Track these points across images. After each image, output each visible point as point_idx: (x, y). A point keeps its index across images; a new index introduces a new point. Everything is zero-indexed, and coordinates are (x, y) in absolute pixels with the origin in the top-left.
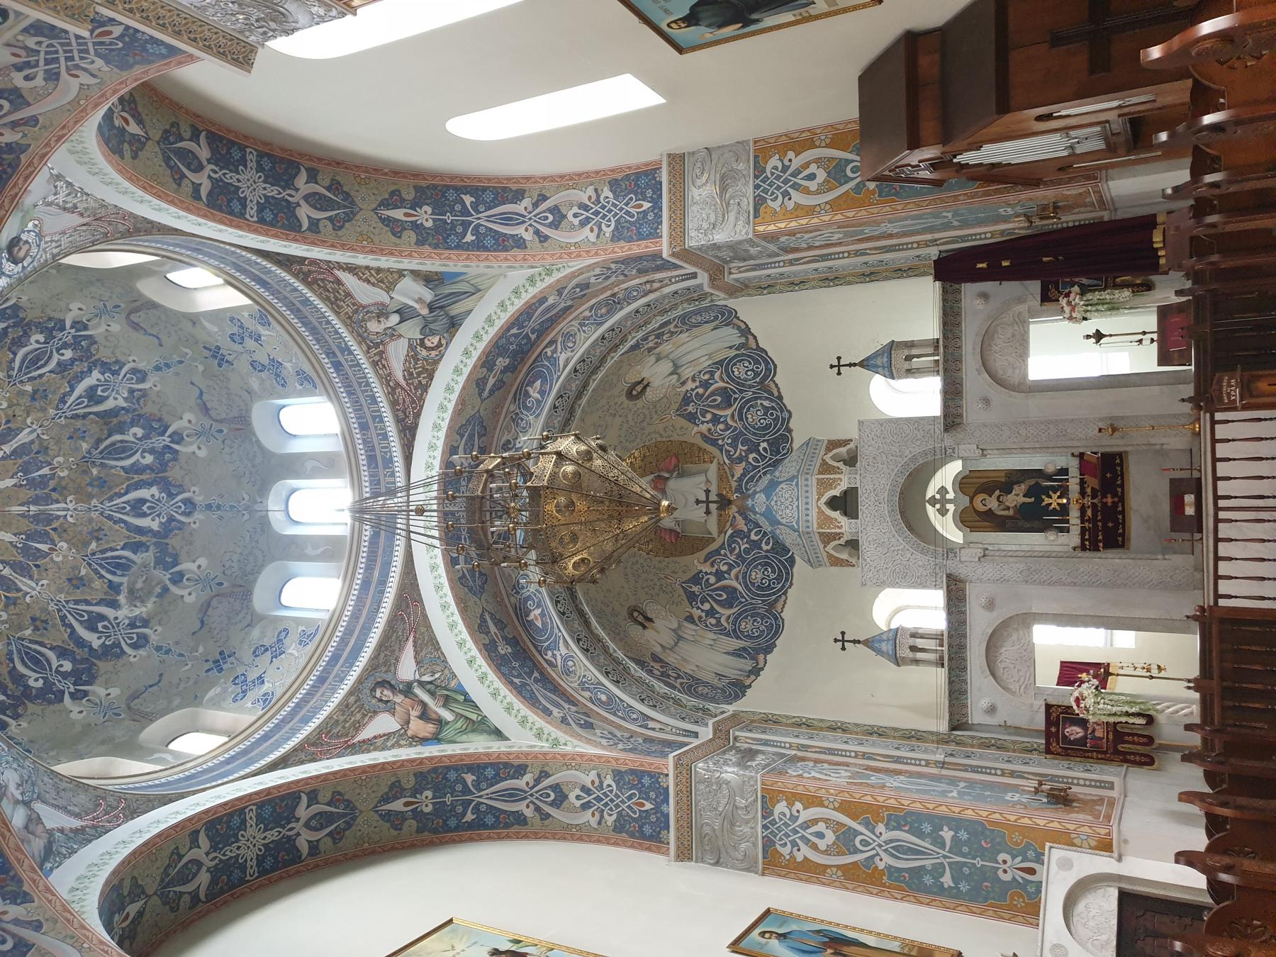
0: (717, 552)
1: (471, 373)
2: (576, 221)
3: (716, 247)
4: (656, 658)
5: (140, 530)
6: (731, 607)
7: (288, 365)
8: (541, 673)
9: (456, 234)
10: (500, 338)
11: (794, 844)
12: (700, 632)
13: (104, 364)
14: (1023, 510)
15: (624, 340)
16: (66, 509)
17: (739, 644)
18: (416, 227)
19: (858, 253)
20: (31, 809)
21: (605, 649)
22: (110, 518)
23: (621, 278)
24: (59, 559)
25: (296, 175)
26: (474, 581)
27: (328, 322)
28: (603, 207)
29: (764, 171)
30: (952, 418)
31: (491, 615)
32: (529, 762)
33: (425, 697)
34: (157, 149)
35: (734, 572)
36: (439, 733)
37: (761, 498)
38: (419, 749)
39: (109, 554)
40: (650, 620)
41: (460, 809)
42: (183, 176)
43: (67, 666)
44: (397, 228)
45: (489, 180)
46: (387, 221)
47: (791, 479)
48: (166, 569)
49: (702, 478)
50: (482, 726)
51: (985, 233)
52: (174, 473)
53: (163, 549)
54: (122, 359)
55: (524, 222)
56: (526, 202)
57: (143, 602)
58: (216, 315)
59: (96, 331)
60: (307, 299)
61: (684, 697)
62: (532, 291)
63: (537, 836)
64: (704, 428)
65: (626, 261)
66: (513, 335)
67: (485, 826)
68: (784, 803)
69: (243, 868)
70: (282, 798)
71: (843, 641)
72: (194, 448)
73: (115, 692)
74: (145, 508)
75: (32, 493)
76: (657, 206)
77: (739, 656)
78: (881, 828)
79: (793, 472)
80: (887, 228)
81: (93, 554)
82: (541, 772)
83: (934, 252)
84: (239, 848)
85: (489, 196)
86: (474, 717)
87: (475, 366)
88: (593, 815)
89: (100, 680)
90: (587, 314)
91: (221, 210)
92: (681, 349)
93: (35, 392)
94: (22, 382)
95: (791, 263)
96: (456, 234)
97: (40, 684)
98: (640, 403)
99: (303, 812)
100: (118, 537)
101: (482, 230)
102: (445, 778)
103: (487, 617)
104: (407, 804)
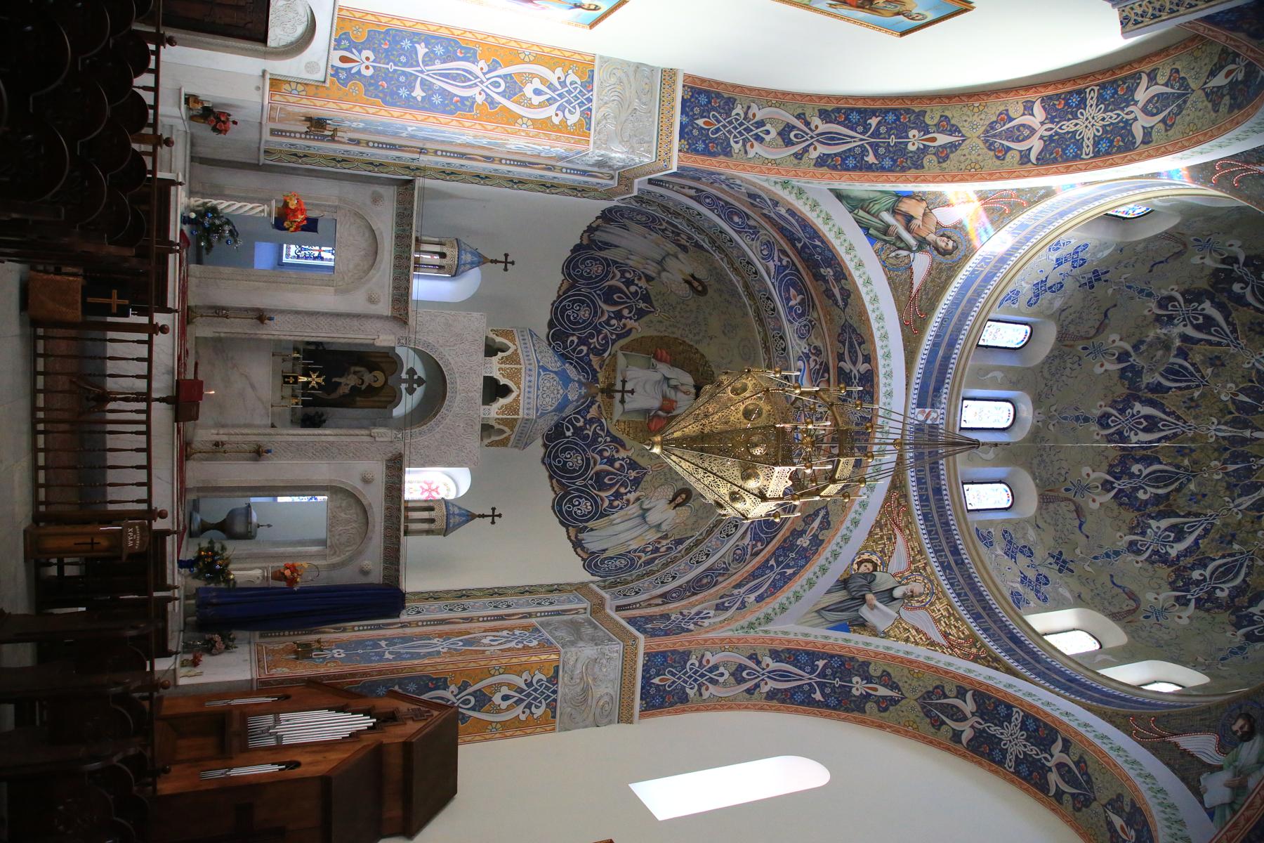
0: (620, 337)
2: (722, 670)
3: (595, 641)
4: (684, 249)
5: (1152, 403)
7: (999, 552)
8: (794, 246)
10: (803, 567)
11: (563, 84)
12: (640, 266)
16: (1215, 430)
17: (603, 254)
18: (868, 679)
19: (469, 620)
21: (731, 263)
22: (1178, 418)
23: (685, 612)
24: (1230, 385)
25: (971, 740)
27: (959, 595)
28: (696, 680)
29: (548, 705)
30: (396, 468)
31: (836, 303)
34: (1097, 795)
35: (604, 318)
37: (572, 396)
40: (687, 282)
41: (883, 130)
42: (1077, 764)
43: (1237, 287)
46: (894, 686)
47: (542, 415)
48: (1132, 366)
49: (628, 406)
53: (1133, 386)
54: (1147, 565)
57: (1158, 338)
58: (1060, 605)
59: (1167, 595)
61: (660, 214)
64: (623, 454)
67: (859, 111)
68: (569, 123)
69: (1101, 99)
70: (1055, 161)
71: (506, 262)
72: (1093, 476)
73: (1196, 260)
74: (1145, 424)
75: (1246, 449)
76: (646, 680)
77: (606, 243)
78: (480, 99)
79: (541, 421)
81: (1198, 386)
83: (404, 617)
84: (1103, 119)
86: (861, 213)
87: (829, 542)
88: (754, 115)
89: (1207, 272)
90: (720, 579)
91: (1045, 724)
92: (639, 532)
93: (1230, 543)
94: (1242, 553)
95: (530, 615)
99: (1036, 145)
100: (1172, 400)
104: (934, 140)
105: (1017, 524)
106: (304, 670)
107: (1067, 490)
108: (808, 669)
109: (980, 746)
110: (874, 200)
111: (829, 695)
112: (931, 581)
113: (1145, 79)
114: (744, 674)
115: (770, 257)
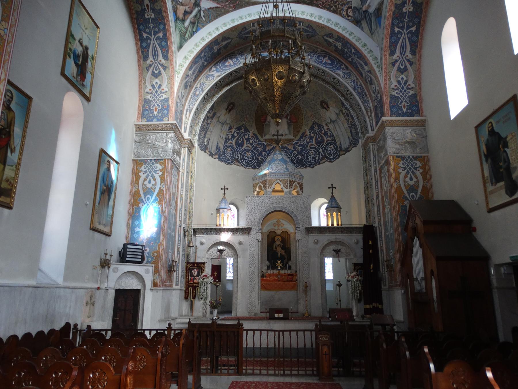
0: (257, 138)
1: (335, 31)
2: (400, 79)
3: (385, 139)
4: (214, 114)
6: (236, 144)
8: (206, 66)
9: (399, 23)
10: (350, 44)
11: (146, 172)
14: (276, 253)
15: (346, 99)
19: (377, 196)
23: (374, 99)
26: (244, 34)
28: (405, 91)
29: (415, 160)
32: (170, 61)
36: (179, 20)
37: (280, 157)
38: (172, 11)
40: (229, 112)
41: (147, 30)
45: (421, 39)
47: (287, 169)
49: (287, 132)
50: (183, 40)
51: (382, 244)
55: (401, 55)
56: (410, 56)
62: (370, 59)
63: (139, 66)
65: (381, 101)
66: (351, 51)
67: (141, 43)
68: (161, 168)
71: (225, 189)
76: (404, 114)
77: (217, 148)
79: (290, 170)
80: (388, 208)
82: (166, 67)
83: (376, 225)
86: (187, 36)
87: (338, 33)
88: (150, 90)
90: (359, 84)
92: (341, 123)
95: (375, 170)
96: (399, 23)
98: (319, 106)
101: (399, 36)
103: (229, 41)
106: (398, 267)
114: (402, 67)
115: (212, 76)
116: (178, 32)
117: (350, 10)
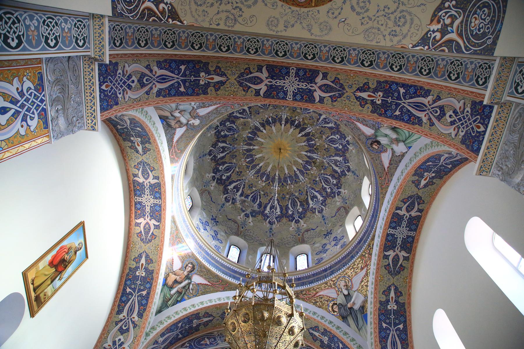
5: (265, 207)
7: (325, 255)
8: (180, 339)
10: (337, 338)
13: (325, 201)
18: (388, 301)
20: (185, 125)
27: (344, 266)
31: (211, 321)
33: (183, 284)
34: (415, 193)
39: (259, 197)
42: (405, 203)
44: (386, 292)
46: (389, 289)
48: (251, 213)
50: (164, 305)
52: (284, 220)
53: (259, 213)
54: (327, 206)
58: (345, 231)
60: (354, 257)
69: (140, 196)
70: (160, 215)
72: (293, 226)
73: (212, 188)
75: (282, 178)
82: (137, 325)
84: (147, 195)
85: (403, 336)
86: (169, 303)
87: (324, 325)
89: (217, 185)
91: (392, 218)
93: (316, 181)
97: (220, 169)
99: (153, 222)
100: (264, 201)
102: (148, 282)
104: (142, 264)
105: (313, 250)
107: (299, 235)
108: (388, 332)
109: (408, 248)
110: (165, 296)
111: (400, 321)
112: (339, 278)
113: (135, 178)
116: (162, 296)
117: (336, 306)
